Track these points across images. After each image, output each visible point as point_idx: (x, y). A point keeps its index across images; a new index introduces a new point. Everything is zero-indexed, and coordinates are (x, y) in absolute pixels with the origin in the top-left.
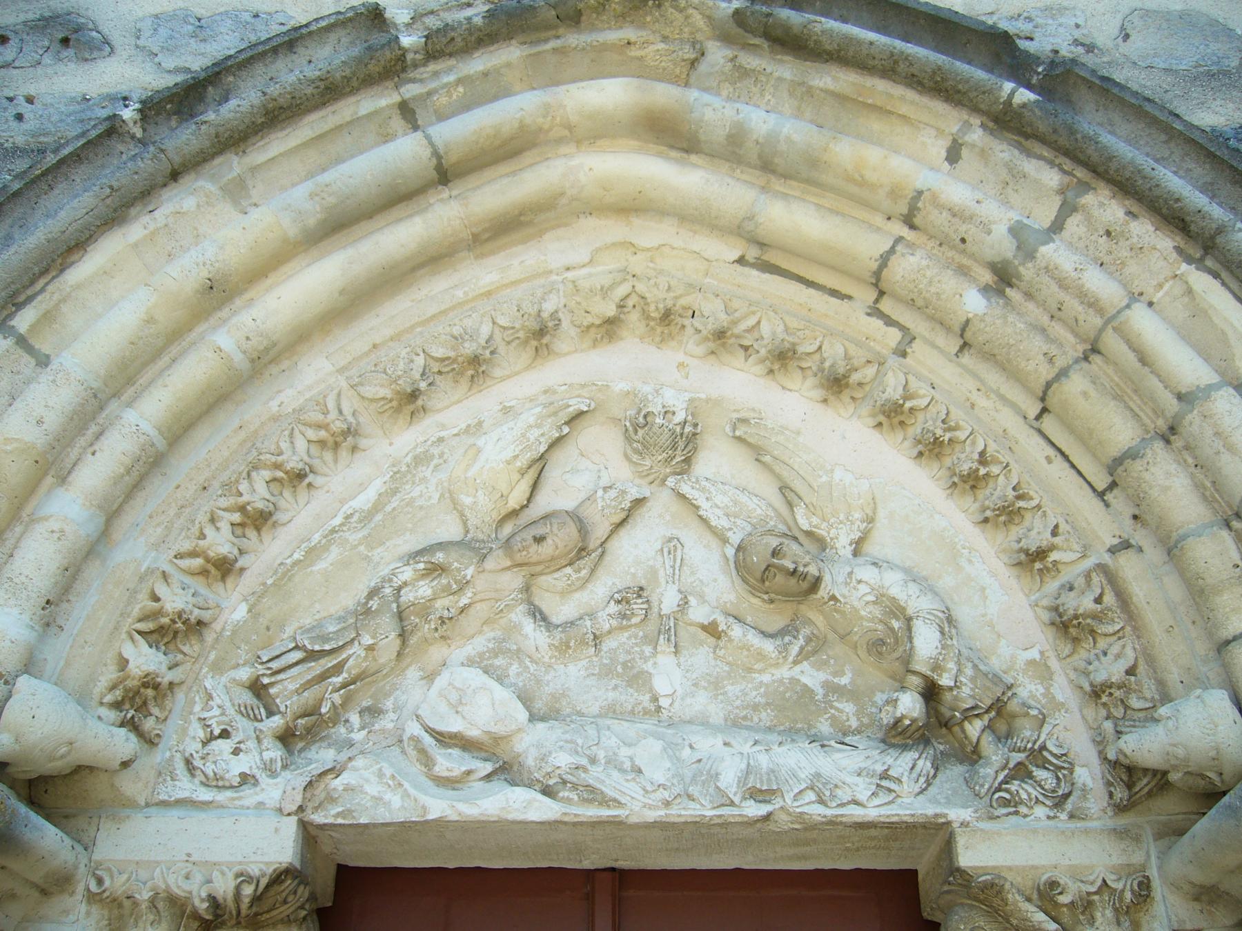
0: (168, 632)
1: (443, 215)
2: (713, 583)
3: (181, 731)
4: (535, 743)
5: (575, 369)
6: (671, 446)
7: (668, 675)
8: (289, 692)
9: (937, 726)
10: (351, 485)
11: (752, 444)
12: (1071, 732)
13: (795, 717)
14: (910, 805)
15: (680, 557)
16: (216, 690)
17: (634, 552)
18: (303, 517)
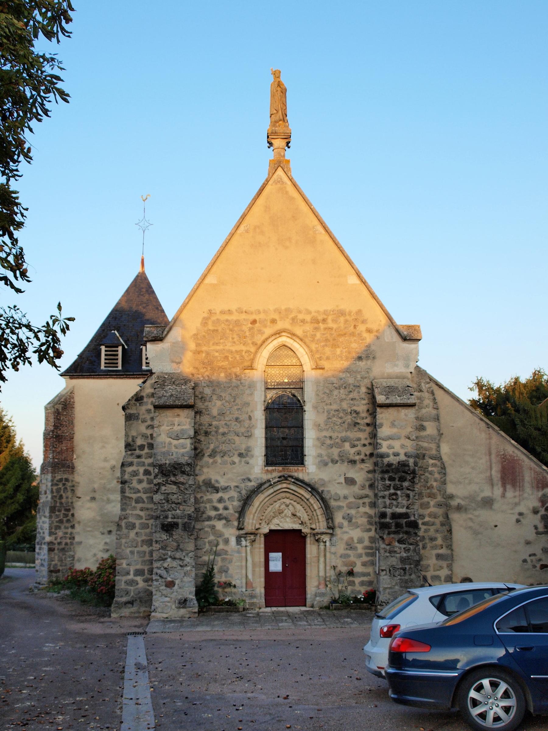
0: (261, 520)
1: (275, 494)
2: (290, 515)
3: (262, 525)
4: (281, 524)
5: (282, 500)
6: (287, 506)
7: (288, 520)
8: (267, 522)
9: (302, 523)
10: (269, 509)
11: (293, 506)
12: (309, 524)
13: (294, 522)
14: (300, 528)
15: (288, 512)
16: (263, 523)
17: (286, 511)
18: (267, 512)
